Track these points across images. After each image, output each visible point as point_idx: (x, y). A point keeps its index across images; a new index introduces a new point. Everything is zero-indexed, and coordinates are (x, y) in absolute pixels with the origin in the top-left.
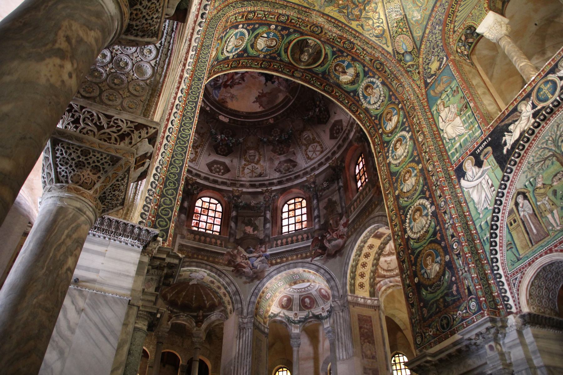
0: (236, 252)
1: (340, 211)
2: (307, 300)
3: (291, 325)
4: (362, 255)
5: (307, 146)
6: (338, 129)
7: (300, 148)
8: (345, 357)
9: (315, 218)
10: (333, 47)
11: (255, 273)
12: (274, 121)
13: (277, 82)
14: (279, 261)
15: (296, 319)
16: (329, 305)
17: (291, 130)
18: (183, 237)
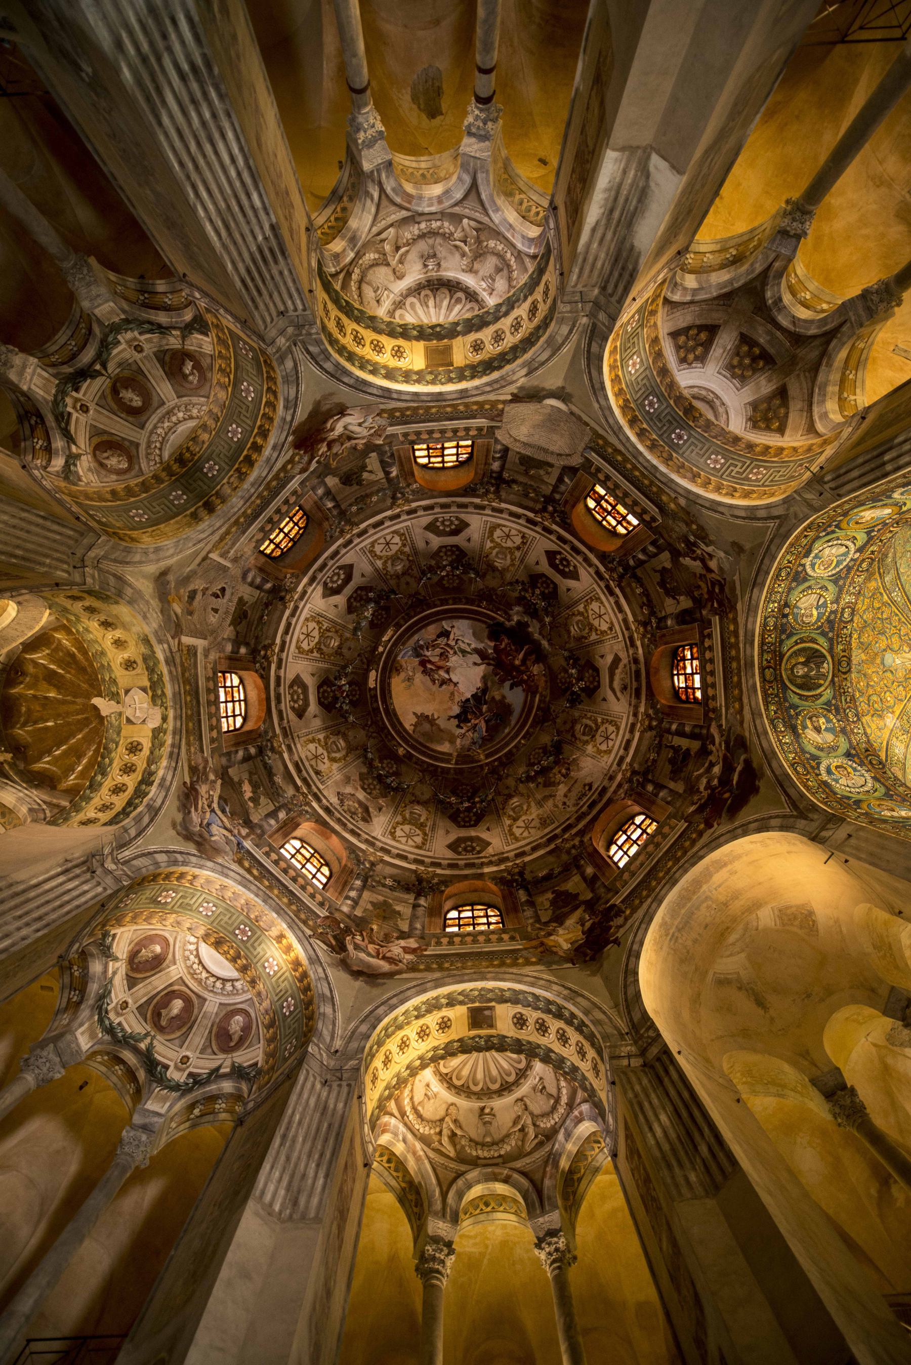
0: (212, 777)
1: (405, 927)
2: (177, 1005)
3: (92, 1016)
4: (421, 1022)
5: (404, 822)
6: (474, 849)
7: (395, 812)
8: (277, 1207)
9: (348, 897)
10: (834, 697)
11: (201, 836)
12: (404, 756)
13: (463, 731)
14: (255, 872)
15: (112, 1015)
16: (214, 1065)
17: (408, 786)
18: (206, 653)
